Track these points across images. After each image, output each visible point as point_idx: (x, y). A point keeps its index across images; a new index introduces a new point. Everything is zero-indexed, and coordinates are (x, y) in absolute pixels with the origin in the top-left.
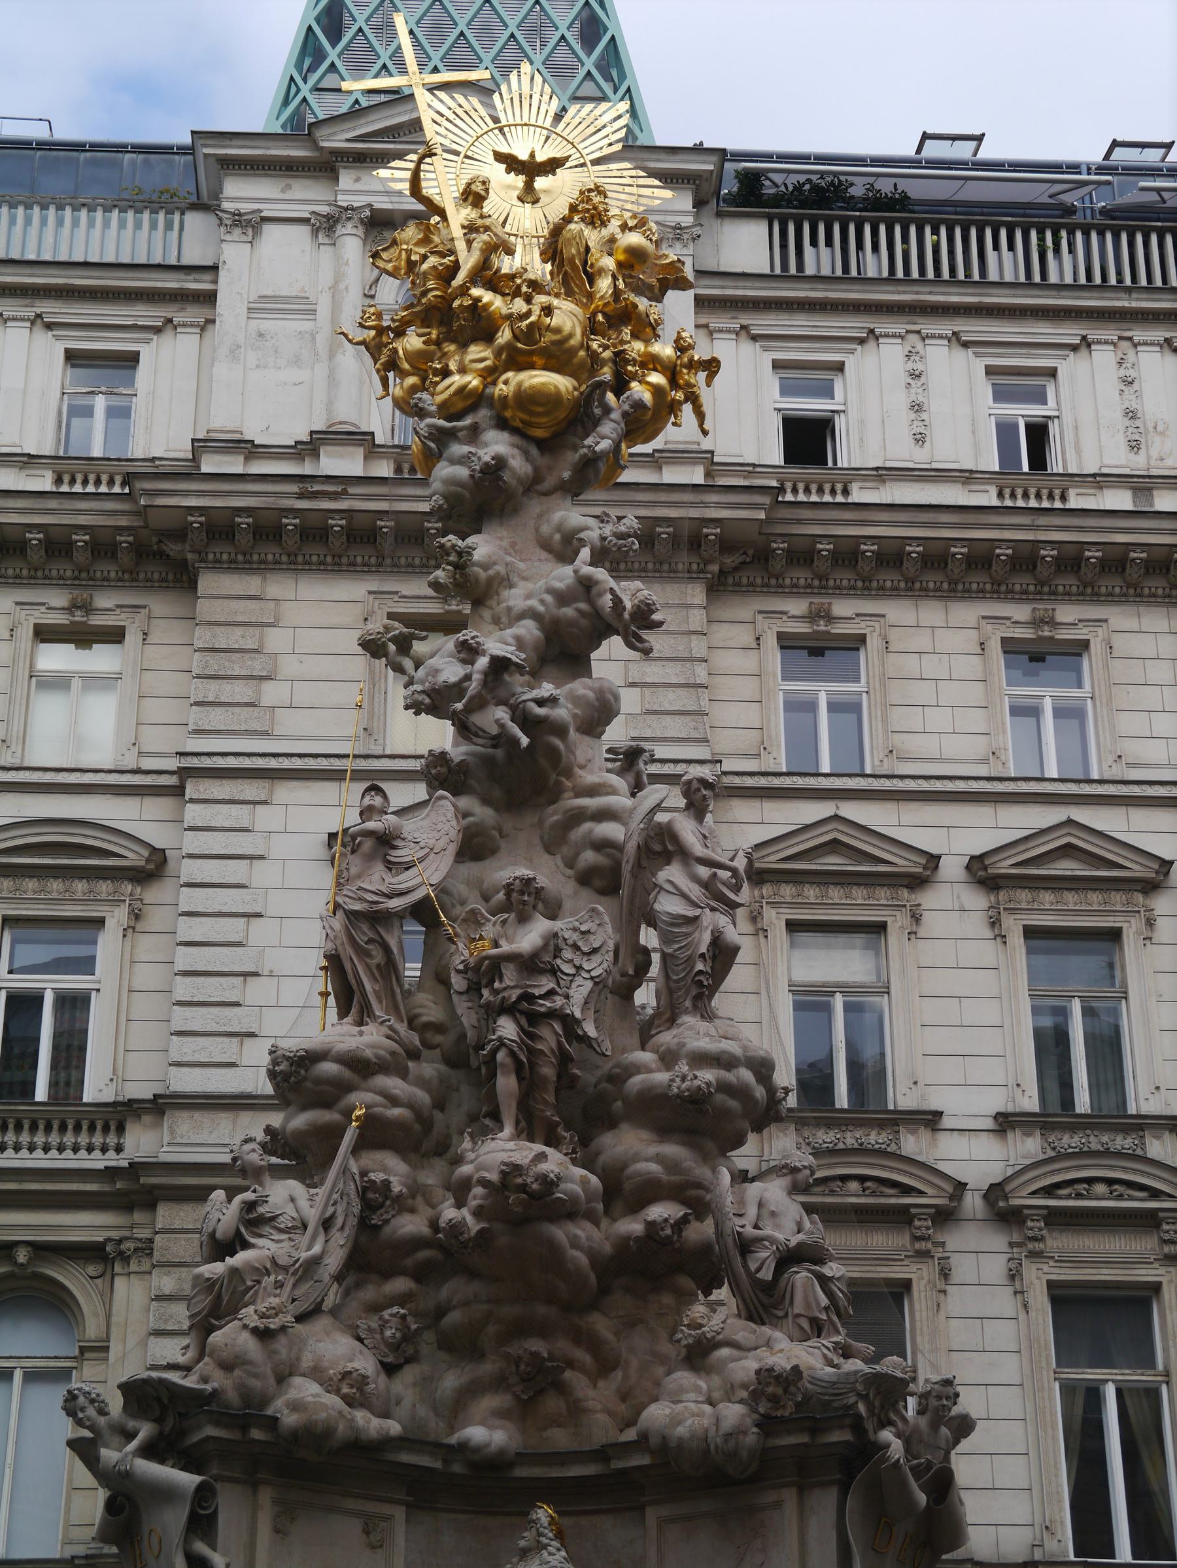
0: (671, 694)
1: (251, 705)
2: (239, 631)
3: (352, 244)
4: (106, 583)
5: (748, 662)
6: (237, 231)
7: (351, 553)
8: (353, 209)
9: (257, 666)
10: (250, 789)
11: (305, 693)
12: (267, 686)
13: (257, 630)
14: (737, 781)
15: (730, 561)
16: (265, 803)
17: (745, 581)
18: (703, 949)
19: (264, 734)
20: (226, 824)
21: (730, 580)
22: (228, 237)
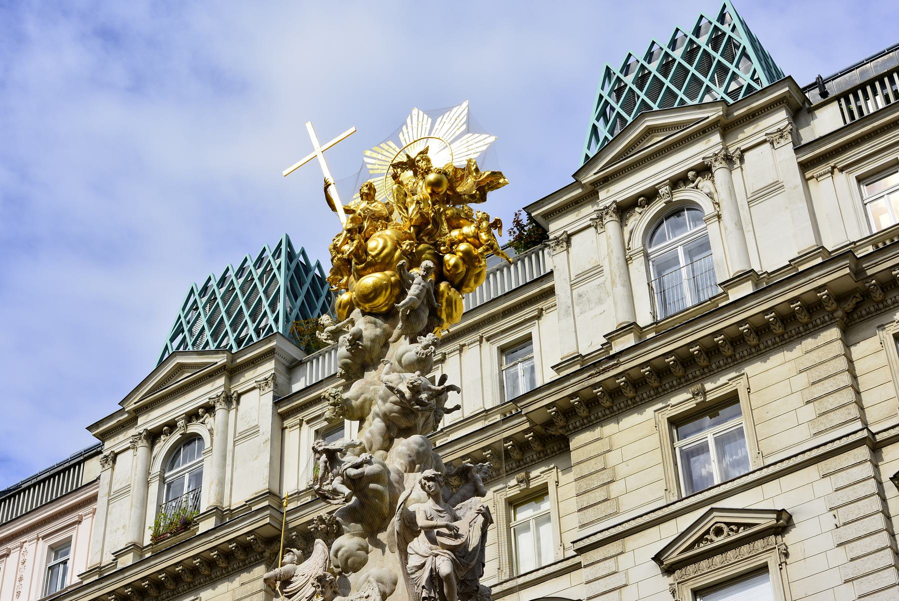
0: (830, 399)
1: (606, 500)
2: (593, 461)
3: (611, 225)
4: (534, 464)
5: (882, 358)
6: (558, 248)
7: (639, 393)
8: (607, 208)
9: (605, 477)
10: (612, 548)
11: (632, 482)
12: (613, 486)
13: (601, 457)
14: (885, 435)
15: (849, 305)
16: (622, 553)
17: (864, 312)
18: (424, 584)
19: (616, 513)
20: (604, 573)
21: (855, 316)
22: (555, 253)
